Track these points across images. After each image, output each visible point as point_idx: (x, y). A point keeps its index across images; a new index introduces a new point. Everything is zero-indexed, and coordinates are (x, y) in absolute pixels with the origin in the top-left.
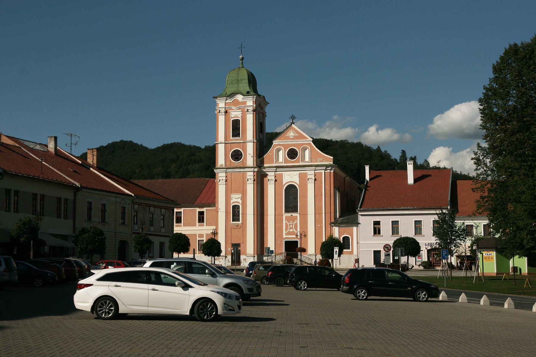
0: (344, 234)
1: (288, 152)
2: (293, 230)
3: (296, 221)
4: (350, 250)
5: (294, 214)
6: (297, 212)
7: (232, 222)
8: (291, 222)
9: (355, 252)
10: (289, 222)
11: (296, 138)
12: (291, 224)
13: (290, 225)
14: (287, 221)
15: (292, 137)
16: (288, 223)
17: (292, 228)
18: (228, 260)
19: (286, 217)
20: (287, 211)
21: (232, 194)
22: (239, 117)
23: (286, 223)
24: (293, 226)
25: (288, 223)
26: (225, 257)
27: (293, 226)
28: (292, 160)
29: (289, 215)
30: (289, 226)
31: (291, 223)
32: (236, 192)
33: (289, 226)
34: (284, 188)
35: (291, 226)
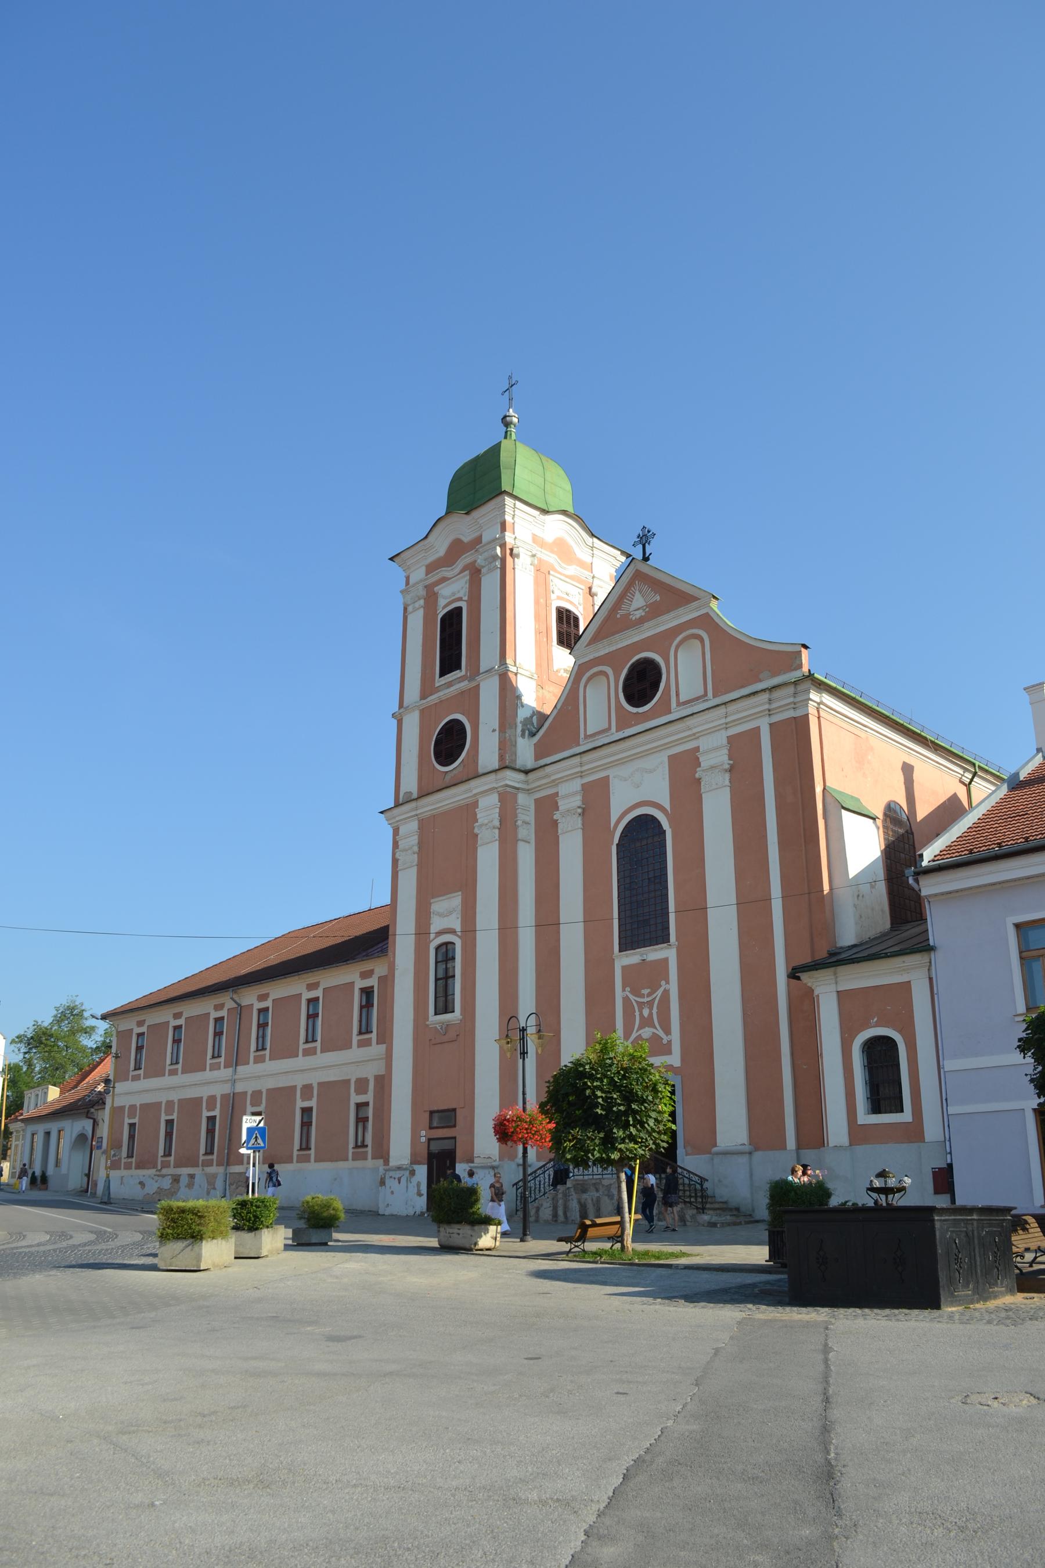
0: (866, 1026)
1: (627, 679)
2: (655, 1031)
3: (663, 983)
4: (906, 1116)
5: (654, 954)
6: (665, 939)
7: (433, 1019)
8: (646, 991)
9: (932, 1130)
10: (636, 992)
11: (654, 611)
12: (645, 1000)
13: (641, 1005)
14: (628, 989)
15: (639, 614)
16: (631, 997)
17: (647, 1022)
18: (419, 1184)
19: (624, 968)
20: (626, 945)
21: (432, 901)
22: (460, 599)
23: (626, 1000)
24: (655, 1011)
25: (631, 997)
26: (407, 1173)
27: (655, 1011)
28: (641, 710)
29: (633, 958)
30: (637, 1013)
31: (642, 996)
32: (445, 890)
33: (637, 1013)
34: (616, 840)
35: (646, 1012)
